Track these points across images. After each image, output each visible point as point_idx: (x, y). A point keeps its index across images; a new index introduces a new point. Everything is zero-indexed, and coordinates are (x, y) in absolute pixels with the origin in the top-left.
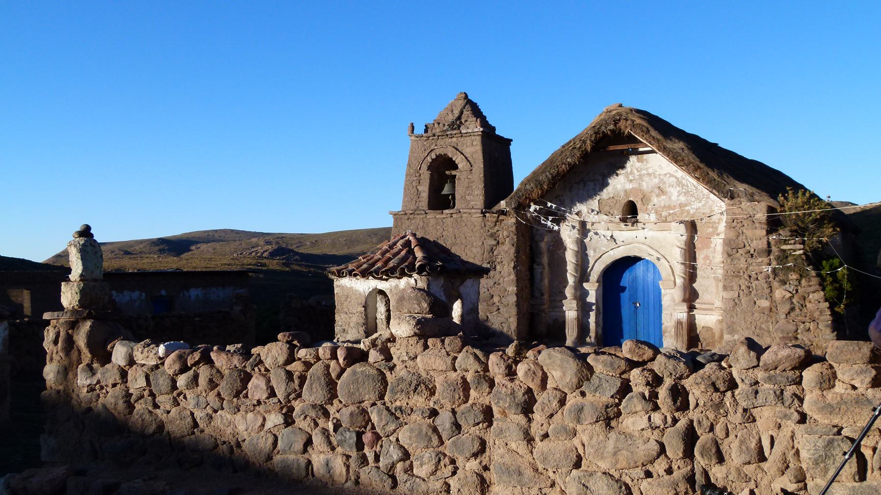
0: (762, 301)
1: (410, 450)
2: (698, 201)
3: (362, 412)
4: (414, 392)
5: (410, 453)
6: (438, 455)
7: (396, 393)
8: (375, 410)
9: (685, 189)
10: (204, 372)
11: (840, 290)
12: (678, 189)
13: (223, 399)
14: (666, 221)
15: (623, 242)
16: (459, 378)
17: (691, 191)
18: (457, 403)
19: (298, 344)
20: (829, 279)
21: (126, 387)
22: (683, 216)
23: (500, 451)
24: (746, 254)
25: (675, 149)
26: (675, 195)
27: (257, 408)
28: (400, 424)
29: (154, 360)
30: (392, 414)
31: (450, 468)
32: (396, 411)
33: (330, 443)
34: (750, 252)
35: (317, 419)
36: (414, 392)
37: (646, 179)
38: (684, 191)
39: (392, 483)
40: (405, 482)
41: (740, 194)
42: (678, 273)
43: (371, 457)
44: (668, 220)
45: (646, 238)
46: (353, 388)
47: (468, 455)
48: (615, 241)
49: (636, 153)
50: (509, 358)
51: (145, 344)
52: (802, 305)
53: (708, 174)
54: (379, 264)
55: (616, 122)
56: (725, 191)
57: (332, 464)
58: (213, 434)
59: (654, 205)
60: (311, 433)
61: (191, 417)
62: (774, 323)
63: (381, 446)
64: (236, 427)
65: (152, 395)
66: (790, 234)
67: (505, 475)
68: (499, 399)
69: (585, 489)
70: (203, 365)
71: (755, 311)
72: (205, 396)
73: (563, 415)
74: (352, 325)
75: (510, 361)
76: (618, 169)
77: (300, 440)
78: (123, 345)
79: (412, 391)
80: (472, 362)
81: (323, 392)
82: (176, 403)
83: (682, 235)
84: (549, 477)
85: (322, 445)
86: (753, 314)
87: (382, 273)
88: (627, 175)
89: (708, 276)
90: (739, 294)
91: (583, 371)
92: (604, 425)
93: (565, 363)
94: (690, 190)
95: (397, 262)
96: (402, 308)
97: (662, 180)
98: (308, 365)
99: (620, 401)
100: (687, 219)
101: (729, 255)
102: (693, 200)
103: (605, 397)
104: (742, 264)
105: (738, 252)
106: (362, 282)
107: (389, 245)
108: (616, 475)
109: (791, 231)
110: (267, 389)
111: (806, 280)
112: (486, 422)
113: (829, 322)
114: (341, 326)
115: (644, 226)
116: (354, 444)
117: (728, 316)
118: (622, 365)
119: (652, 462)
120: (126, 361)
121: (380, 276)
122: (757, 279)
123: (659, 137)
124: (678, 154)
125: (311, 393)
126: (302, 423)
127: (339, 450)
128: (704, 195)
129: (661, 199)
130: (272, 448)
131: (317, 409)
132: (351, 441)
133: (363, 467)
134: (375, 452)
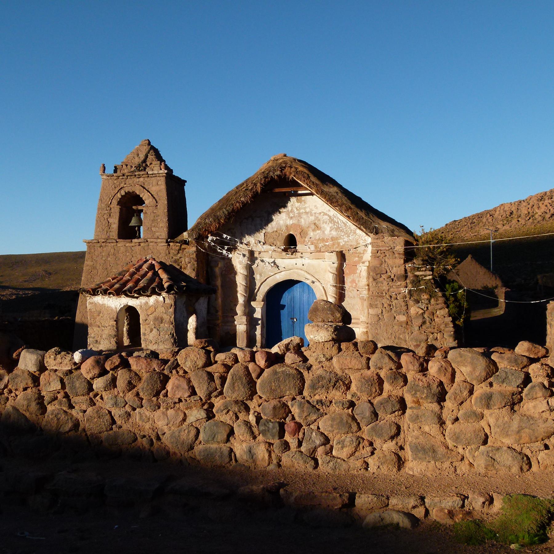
0: (400, 316)
1: (330, 436)
2: (346, 235)
3: (284, 406)
4: (333, 388)
5: (329, 438)
6: (358, 439)
7: (316, 389)
8: (296, 403)
9: (336, 225)
10: (122, 376)
11: (460, 307)
12: (330, 225)
13: (142, 399)
14: (320, 251)
15: (284, 268)
16: (375, 375)
17: (341, 227)
18: (373, 395)
19: (212, 350)
20: (452, 299)
21: (39, 390)
22: (334, 248)
23: (414, 434)
24: (388, 278)
25: (331, 193)
26: (328, 230)
27: (177, 405)
28: (321, 415)
29: (69, 365)
30: (313, 406)
31: (369, 449)
32: (317, 404)
33: (252, 433)
34: (391, 276)
35: (239, 413)
36: (333, 388)
37: (304, 216)
38: (336, 227)
39: (314, 464)
40: (327, 463)
41: (383, 230)
42: (330, 294)
43: (293, 443)
44: (322, 250)
45: (303, 265)
46: (274, 386)
47: (386, 438)
48: (278, 267)
49: (296, 195)
50: (420, 357)
51: (57, 352)
52: (431, 320)
53: (358, 213)
54: (130, 285)
55: (282, 169)
56: (371, 227)
57: (255, 451)
58: (131, 429)
59: (310, 238)
60: (232, 425)
61: (109, 415)
62: (410, 334)
63: (304, 434)
64: (155, 422)
65: (67, 396)
66: (422, 262)
67: (421, 453)
68: (416, 391)
69: (493, 461)
70: (121, 369)
71: (394, 324)
72: (122, 396)
73: (471, 402)
74: (104, 336)
75: (421, 360)
76: (281, 208)
77: (223, 432)
78: (31, 353)
79: (332, 387)
80: (387, 361)
81: (245, 390)
82: (92, 403)
83: (333, 263)
84: (459, 453)
85: (245, 435)
86: (394, 327)
87: (135, 292)
88: (288, 213)
89: (354, 297)
90: (382, 311)
91: (490, 366)
92: (509, 409)
93: (475, 360)
94: (340, 226)
95: (146, 282)
96: (316, 318)
97: (317, 217)
98: (228, 368)
99: (522, 389)
100: (337, 250)
101: (374, 280)
102: (343, 234)
103: (511, 387)
104: (385, 287)
105: (381, 277)
106: (114, 299)
107: (136, 268)
108: (518, 449)
109: (423, 260)
110: (189, 388)
111: (434, 300)
112: (401, 410)
113: (452, 333)
114: (94, 338)
115: (301, 255)
116: (277, 433)
117: (373, 329)
118: (524, 361)
119: (549, 437)
120: (37, 367)
121: (133, 294)
122: (397, 298)
123: (317, 182)
124: (333, 197)
125: (233, 391)
126: (221, 417)
127: (260, 438)
128: (351, 230)
129: (316, 233)
130: (194, 439)
131: (239, 405)
132: (275, 431)
133: (286, 452)
134: (298, 439)
